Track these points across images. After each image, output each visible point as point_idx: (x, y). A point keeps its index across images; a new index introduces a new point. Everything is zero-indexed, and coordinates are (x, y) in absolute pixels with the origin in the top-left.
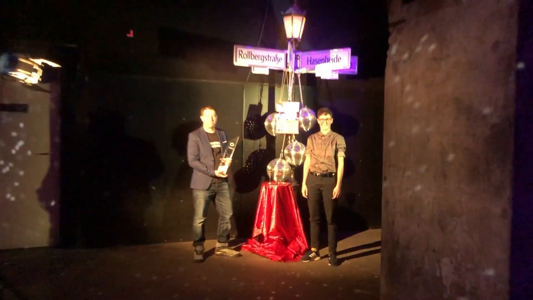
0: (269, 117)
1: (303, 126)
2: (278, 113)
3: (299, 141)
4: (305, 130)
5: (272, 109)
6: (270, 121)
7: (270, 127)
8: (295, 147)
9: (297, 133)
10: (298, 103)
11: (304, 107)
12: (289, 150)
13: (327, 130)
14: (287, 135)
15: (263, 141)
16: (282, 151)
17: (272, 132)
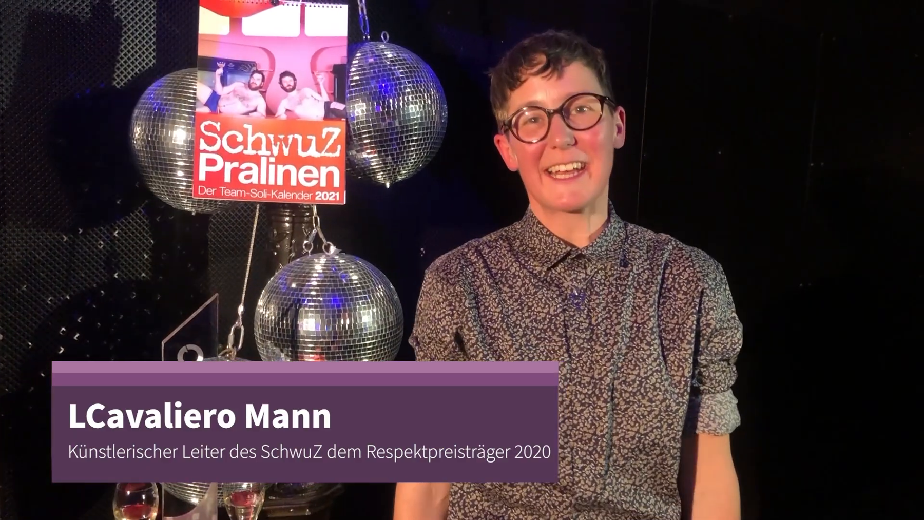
0: (155, 92)
1: (370, 157)
2: (210, 64)
3: (344, 248)
4: (380, 176)
5: (179, 49)
6: (160, 117)
9: (336, 197)
10: (343, 11)
11: (376, 38)
12: (291, 309)
14: (272, 210)
15: (131, 235)
16: (241, 309)
17: (171, 185)
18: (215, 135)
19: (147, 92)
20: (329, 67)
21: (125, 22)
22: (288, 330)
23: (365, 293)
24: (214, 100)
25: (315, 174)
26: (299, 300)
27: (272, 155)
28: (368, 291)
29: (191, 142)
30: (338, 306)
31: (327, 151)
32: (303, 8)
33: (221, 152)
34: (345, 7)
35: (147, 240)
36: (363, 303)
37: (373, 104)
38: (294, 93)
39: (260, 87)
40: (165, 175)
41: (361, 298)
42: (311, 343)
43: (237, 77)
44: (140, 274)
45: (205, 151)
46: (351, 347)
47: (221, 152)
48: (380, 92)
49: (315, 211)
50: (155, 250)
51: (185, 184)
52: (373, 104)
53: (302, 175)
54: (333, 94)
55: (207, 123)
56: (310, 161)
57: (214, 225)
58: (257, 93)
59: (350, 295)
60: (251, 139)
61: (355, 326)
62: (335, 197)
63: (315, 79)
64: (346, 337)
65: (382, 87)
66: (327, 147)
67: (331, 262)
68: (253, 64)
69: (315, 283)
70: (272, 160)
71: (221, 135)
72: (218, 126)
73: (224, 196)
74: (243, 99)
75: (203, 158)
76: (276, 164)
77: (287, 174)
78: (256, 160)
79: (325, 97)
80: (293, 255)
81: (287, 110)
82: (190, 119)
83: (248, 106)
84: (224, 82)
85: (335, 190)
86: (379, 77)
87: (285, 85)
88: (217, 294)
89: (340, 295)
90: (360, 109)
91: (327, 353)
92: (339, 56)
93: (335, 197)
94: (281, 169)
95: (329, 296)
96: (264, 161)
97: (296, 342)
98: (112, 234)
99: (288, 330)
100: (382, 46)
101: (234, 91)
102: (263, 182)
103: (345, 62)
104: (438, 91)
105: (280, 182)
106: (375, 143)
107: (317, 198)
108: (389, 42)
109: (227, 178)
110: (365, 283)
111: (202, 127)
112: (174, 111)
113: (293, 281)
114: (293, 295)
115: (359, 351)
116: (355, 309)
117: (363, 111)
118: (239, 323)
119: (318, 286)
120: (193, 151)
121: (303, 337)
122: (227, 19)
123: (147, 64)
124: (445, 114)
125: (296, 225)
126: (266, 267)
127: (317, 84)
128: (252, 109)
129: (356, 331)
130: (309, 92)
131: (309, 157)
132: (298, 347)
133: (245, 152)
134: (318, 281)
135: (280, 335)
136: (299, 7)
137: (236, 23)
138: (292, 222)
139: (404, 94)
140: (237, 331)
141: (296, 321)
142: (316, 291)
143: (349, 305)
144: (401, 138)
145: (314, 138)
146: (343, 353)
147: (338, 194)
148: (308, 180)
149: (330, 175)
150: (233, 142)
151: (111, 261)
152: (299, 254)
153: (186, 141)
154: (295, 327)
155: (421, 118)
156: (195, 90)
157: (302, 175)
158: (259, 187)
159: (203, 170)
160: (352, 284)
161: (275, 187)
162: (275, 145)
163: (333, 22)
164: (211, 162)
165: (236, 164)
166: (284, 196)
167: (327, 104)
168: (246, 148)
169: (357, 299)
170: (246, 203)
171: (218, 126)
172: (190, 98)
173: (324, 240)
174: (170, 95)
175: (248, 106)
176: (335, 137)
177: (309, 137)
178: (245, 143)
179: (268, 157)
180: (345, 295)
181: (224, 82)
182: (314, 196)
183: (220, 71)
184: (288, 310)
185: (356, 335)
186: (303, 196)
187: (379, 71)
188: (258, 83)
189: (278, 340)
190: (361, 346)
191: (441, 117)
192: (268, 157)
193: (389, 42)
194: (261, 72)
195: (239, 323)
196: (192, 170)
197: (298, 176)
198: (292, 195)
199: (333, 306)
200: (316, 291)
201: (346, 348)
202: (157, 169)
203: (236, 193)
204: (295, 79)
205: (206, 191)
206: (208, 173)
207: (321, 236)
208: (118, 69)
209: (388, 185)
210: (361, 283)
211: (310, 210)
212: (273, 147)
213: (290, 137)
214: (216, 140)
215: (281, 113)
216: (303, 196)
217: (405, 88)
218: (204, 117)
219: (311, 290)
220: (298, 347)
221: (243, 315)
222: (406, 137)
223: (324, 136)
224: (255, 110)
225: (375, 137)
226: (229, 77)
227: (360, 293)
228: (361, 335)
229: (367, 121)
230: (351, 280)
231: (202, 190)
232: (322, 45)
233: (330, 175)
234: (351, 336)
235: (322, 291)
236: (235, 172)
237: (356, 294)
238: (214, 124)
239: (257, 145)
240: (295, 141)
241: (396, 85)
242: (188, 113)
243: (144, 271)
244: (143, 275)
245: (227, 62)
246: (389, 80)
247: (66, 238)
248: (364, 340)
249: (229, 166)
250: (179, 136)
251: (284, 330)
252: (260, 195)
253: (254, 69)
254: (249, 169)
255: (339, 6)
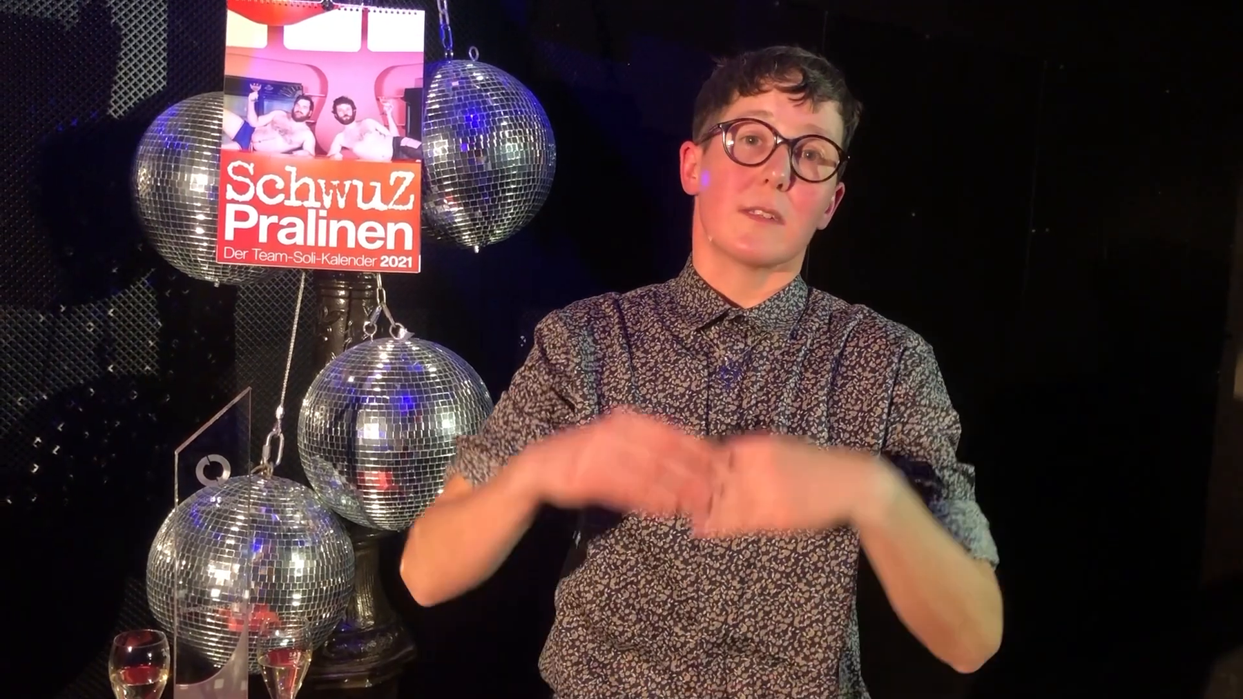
1: (452, 210)
2: (241, 87)
3: (418, 332)
4: (466, 237)
5: (199, 66)
6: (173, 157)
7: (176, 215)
8: (388, 380)
9: (408, 263)
10: (417, 18)
11: (462, 55)
12: (347, 411)
13: (759, 266)
14: (322, 280)
15: (132, 312)
16: (280, 411)
17: (187, 247)
18: (247, 181)
19: (156, 122)
20: (399, 92)
21: (125, 30)
22: (343, 439)
23: (445, 389)
24: (246, 134)
25: (380, 232)
26: (358, 399)
27: (323, 207)
28: (449, 387)
29: (215, 189)
30: (410, 407)
31: (396, 203)
32: (365, 13)
33: (255, 202)
34: (421, 14)
35: (153, 321)
36: (443, 403)
37: (457, 141)
38: (354, 123)
39: (308, 117)
40: (179, 232)
41: (441, 397)
42: (373, 455)
43: (276, 104)
44: (143, 367)
45: (233, 201)
46: (427, 461)
47: (255, 202)
48: (468, 126)
49: (379, 282)
50: (164, 335)
51: (205, 244)
52: (457, 141)
53: (363, 233)
54: (405, 127)
55: (236, 164)
56: (374, 215)
57: (243, 302)
58: (303, 125)
59: (426, 392)
60: (294, 186)
61: (432, 432)
62: (407, 263)
63: (381, 107)
64: (421, 448)
65: (470, 120)
66: (396, 197)
67: (401, 350)
68: (299, 87)
69: (379, 377)
70: (323, 213)
71: (255, 180)
72: (251, 168)
73: (259, 261)
74: (284, 132)
75: (231, 209)
76: (328, 218)
77: (342, 233)
78: (302, 213)
79: (394, 131)
80: (349, 340)
81: (344, 148)
82: (214, 158)
83: (291, 142)
84: (259, 110)
85: (407, 254)
86: (465, 105)
87: (341, 114)
88: (249, 388)
89: (412, 393)
90: (439, 148)
91: (395, 469)
92: (412, 78)
93: (407, 263)
94: (335, 225)
95: (398, 393)
96: (312, 215)
97: (354, 454)
98: (105, 312)
99: (343, 439)
100: (470, 66)
101: (273, 122)
102: (311, 242)
103: (421, 85)
104: (544, 126)
105: (333, 243)
106: (461, 192)
107: (383, 265)
108: (479, 60)
109: (263, 237)
110: (446, 376)
111: (230, 169)
112: (191, 147)
113: (351, 373)
114: (350, 392)
115: (438, 466)
116: (433, 411)
117: (444, 151)
118: (277, 430)
119: (383, 380)
120: (217, 201)
121: (364, 448)
122: (264, 28)
123: (155, 87)
124: (554, 156)
125: (354, 302)
126: (313, 356)
127: (384, 114)
128: (297, 146)
129: (434, 440)
130: (372, 124)
131: (373, 209)
132: (356, 461)
133: (287, 203)
134: (383, 374)
135: (332, 445)
136: (360, 13)
137: (276, 33)
138: (349, 298)
139: (499, 129)
140: (275, 441)
141: (354, 427)
142: (382, 386)
143: (424, 406)
144: (495, 186)
145: (378, 185)
146: (417, 468)
147: (410, 259)
148: (371, 240)
149: (400, 235)
150: (270, 189)
151: (104, 349)
152: (358, 340)
153: (207, 188)
154: (352, 434)
155: (522, 160)
156: (220, 120)
157: (363, 233)
158: (305, 249)
159: (231, 227)
160: (428, 379)
161: (327, 249)
162: (327, 193)
163: (404, 31)
164: (242, 216)
165: (274, 219)
166: (339, 262)
167: (396, 141)
168: (288, 197)
169: (435, 398)
170: (290, 271)
171: (251, 168)
172: (214, 131)
173: (392, 321)
174: (187, 126)
175: (291, 142)
176: (406, 183)
177: (372, 184)
178: (286, 191)
179: (317, 210)
180: (420, 392)
181: (259, 110)
182: (378, 262)
183: (254, 96)
184: (343, 412)
185: (434, 446)
186: (364, 262)
187: (466, 98)
188: (305, 112)
189: (329, 452)
190: (440, 459)
191: (547, 160)
192: (317, 210)
193: (479, 60)
194: (308, 98)
195: (277, 430)
196: (215, 226)
197: (358, 235)
198: (348, 260)
199: (403, 407)
200: (382, 386)
201: (420, 461)
202: (168, 224)
203: (274, 257)
204: (354, 108)
205: (235, 254)
206: (236, 230)
207: (388, 314)
208: (116, 92)
209: (477, 249)
210: (440, 377)
211: (373, 281)
212: (324, 196)
213: (347, 184)
214: (248, 186)
215: (335, 152)
216: (364, 262)
217: (500, 121)
218: (232, 156)
219: (373, 386)
220: (356, 461)
221: (282, 419)
222: (502, 185)
223: (392, 182)
224: (301, 148)
225: (461, 184)
226: (266, 103)
227: (440, 390)
228: (440, 445)
229: (450, 164)
230: (428, 373)
231: (229, 253)
232: (390, 63)
233: (400, 235)
234: (427, 446)
235: (388, 387)
236: (273, 229)
237: (434, 391)
238: (246, 165)
239: (302, 193)
240: (353, 189)
241: (488, 116)
242: (210, 150)
243: (148, 363)
244: (148, 368)
245: (264, 83)
246: (479, 110)
247: (42, 318)
248: (444, 452)
249: (265, 222)
250: (198, 181)
251: (337, 439)
252: (307, 259)
253: (299, 93)
254: (292, 225)
255: (413, 12)
